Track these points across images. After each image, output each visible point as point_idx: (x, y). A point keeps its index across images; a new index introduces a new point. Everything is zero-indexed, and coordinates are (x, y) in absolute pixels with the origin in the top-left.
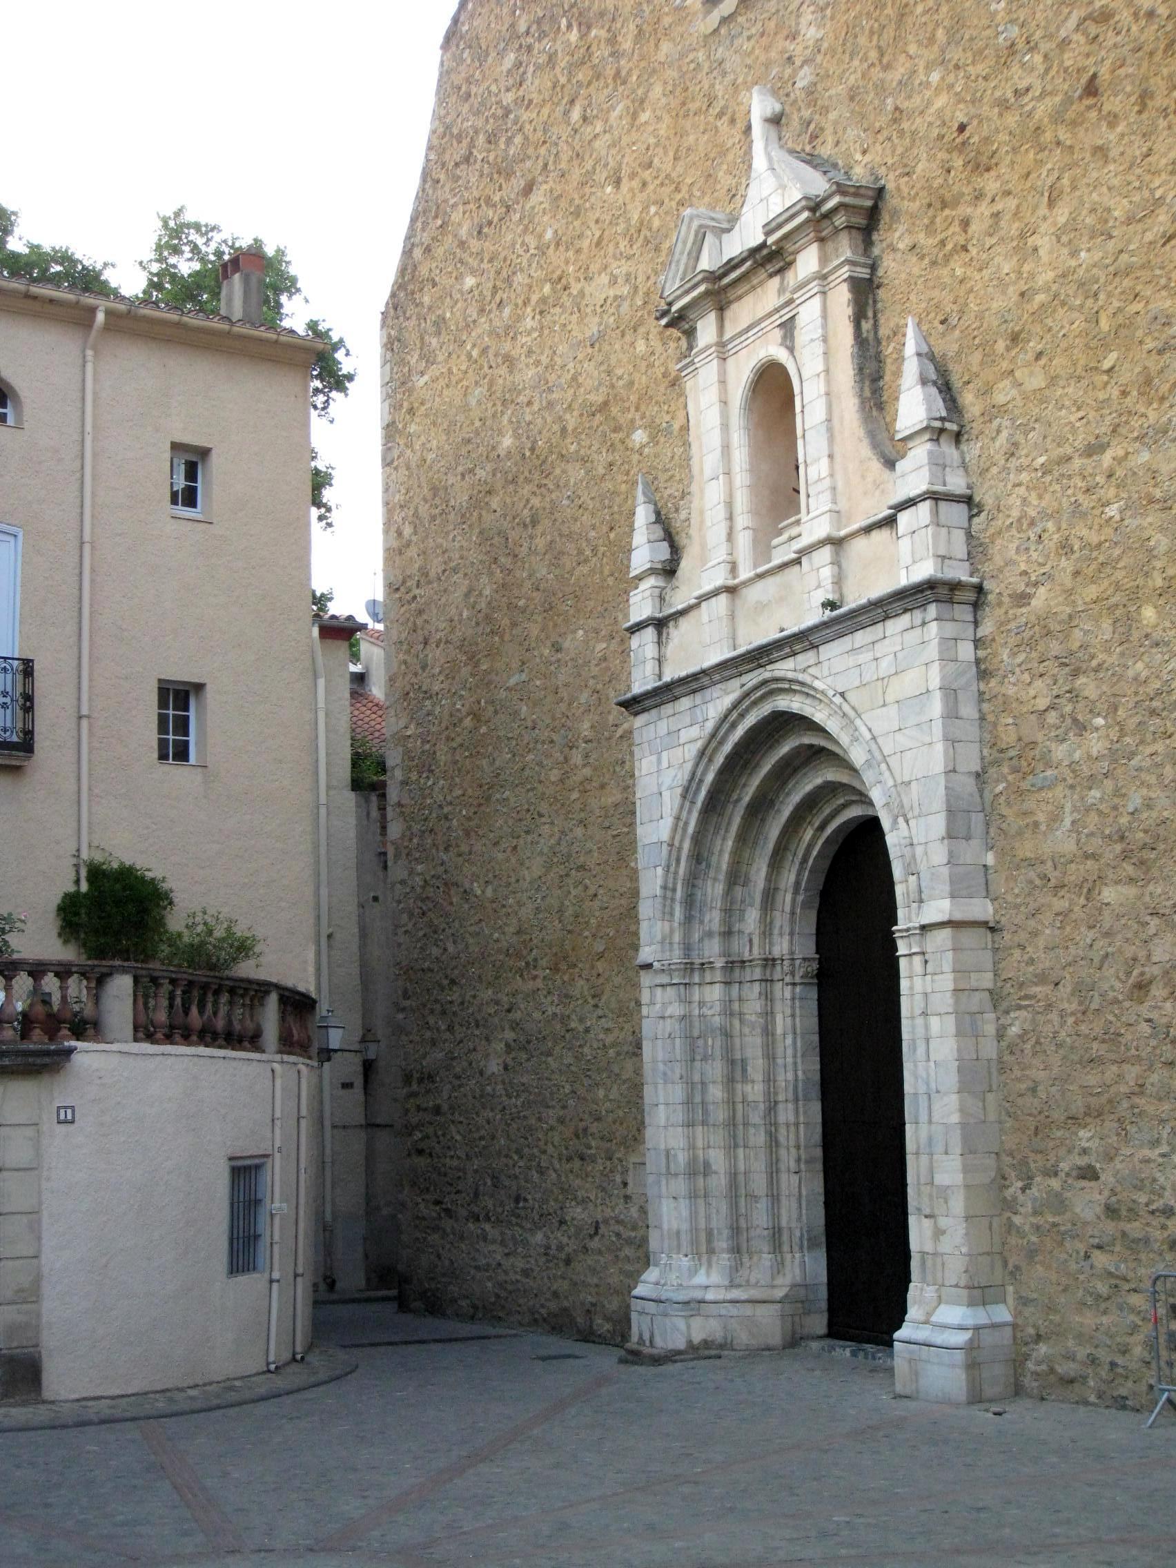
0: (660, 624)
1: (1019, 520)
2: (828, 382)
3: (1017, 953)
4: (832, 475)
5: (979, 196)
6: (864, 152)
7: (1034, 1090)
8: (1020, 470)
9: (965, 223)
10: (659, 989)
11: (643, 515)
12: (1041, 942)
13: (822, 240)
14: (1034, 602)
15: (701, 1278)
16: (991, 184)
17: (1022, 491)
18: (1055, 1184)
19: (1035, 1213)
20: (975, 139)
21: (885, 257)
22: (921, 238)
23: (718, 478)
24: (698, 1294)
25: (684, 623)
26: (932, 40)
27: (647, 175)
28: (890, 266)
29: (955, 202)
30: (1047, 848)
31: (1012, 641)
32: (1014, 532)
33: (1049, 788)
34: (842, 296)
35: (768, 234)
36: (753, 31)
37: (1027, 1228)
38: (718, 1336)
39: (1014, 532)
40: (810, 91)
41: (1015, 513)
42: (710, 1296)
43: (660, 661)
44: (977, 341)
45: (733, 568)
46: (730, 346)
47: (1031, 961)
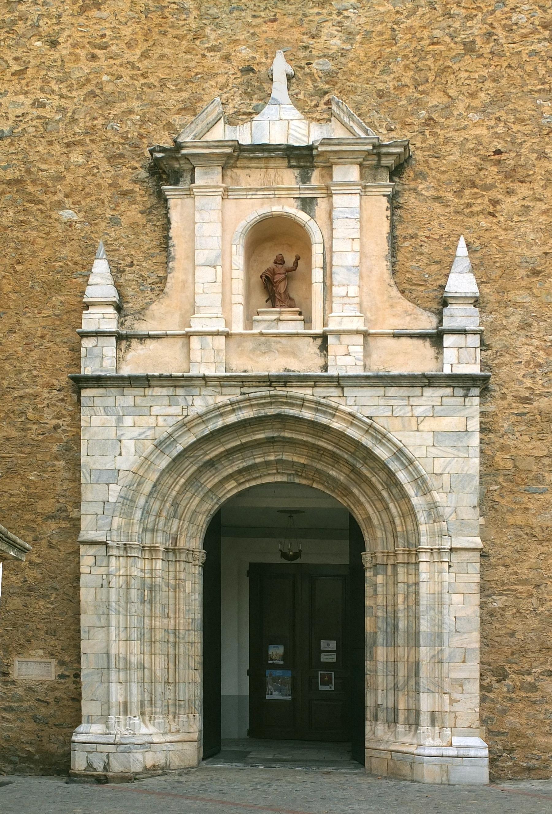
0: (119, 337)
1: (528, 362)
2: (362, 246)
3: (503, 569)
4: (360, 297)
5: (510, 192)
6: (391, 130)
7: (512, 634)
8: (531, 337)
9: (495, 202)
10: (114, 558)
11: (101, 266)
12: (526, 565)
13: (361, 165)
14: (535, 403)
15: (144, 730)
16: (523, 190)
17: (531, 348)
18: (529, 679)
19: (509, 692)
20: (512, 162)
21: (406, 194)
22: (450, 196)
23: (215, 267)
24: (148, 739)
25: (151, 345)
26: (472, 95)
27: (98, 52)
28: (409, 200)
29: (487, 188)
30: (536, 522)
31: (513, 418)
32: (522, 366)
33: (542, 493)
34: (384, 203)
35: (322, 144)
36: (262, 14)
37: (500, 699)
38: (162, 762)
39: (522, 366)
40: (330, 77)
41: (525, 358)
42: (155, 739)
43: (119, 360)
44: (498, 264)
45: (227, 324)
46: (230, 193)
47: (516, 573)
